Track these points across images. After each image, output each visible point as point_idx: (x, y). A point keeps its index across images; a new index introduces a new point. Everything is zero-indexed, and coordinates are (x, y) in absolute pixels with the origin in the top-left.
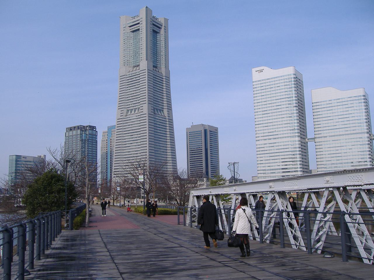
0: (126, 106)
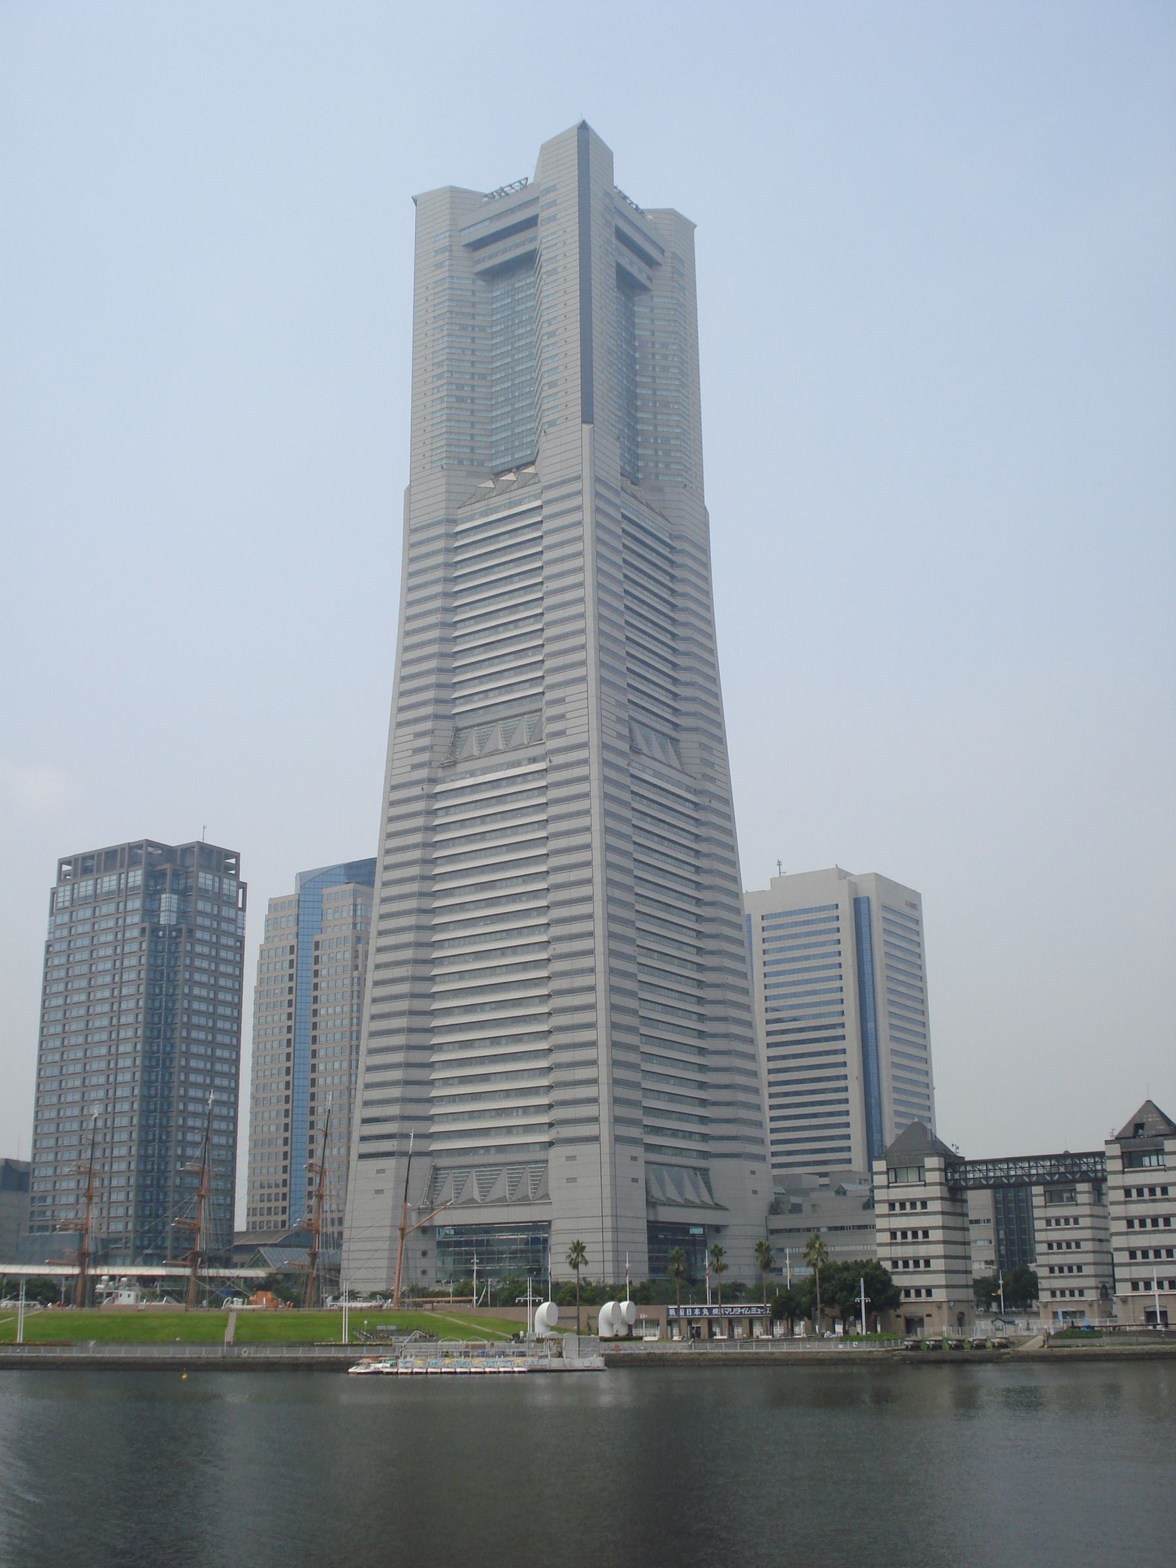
0: (441, 715)
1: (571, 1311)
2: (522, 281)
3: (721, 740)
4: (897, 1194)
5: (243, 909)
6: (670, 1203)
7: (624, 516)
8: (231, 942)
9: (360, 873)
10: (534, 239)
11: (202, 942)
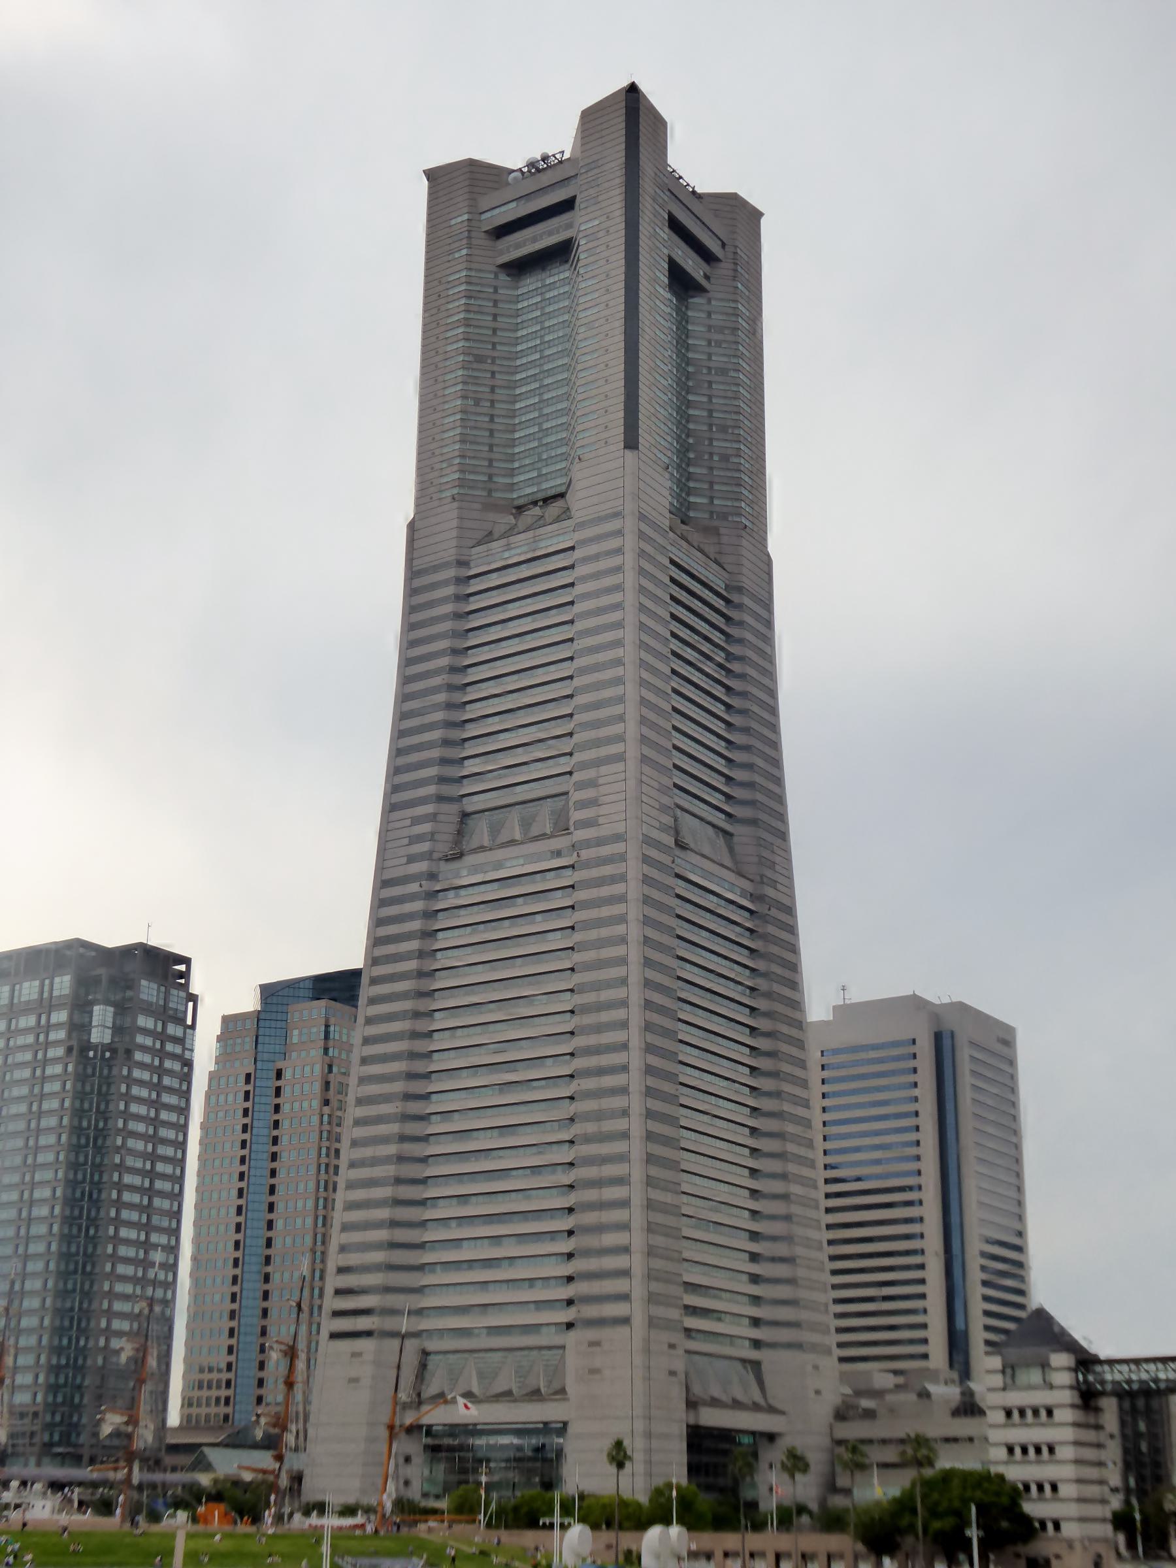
1: (708, 1540)
2: (557, 275)
3: (783, 836)
4: (1015, 1398)
5: (193, 1027)
6: (715, 1402)
7: (672, 562)
9: (338, 988)
10: (570, 226)
11: (142, 1066)
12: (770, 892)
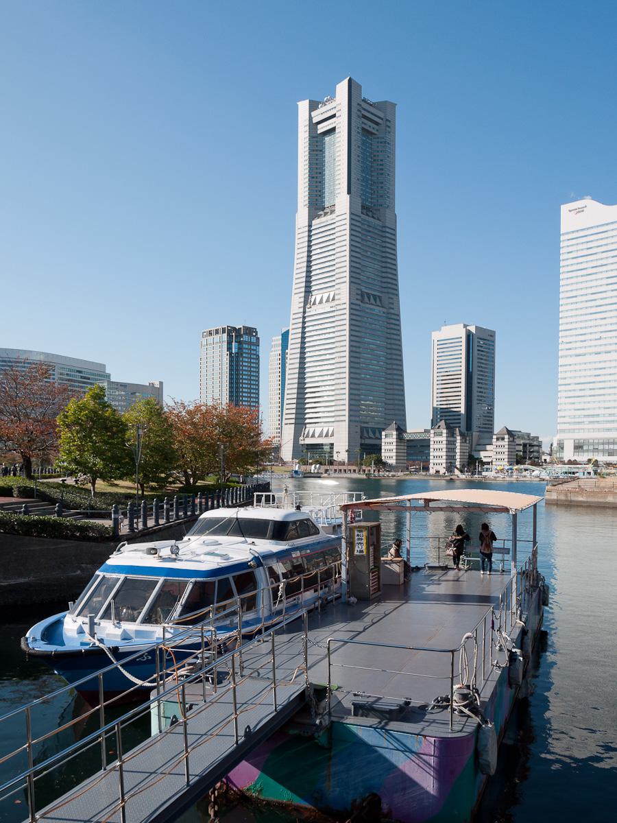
3: (397, 295)
8: (255, 357)
11: (246, 357)
12: (392, 311)
